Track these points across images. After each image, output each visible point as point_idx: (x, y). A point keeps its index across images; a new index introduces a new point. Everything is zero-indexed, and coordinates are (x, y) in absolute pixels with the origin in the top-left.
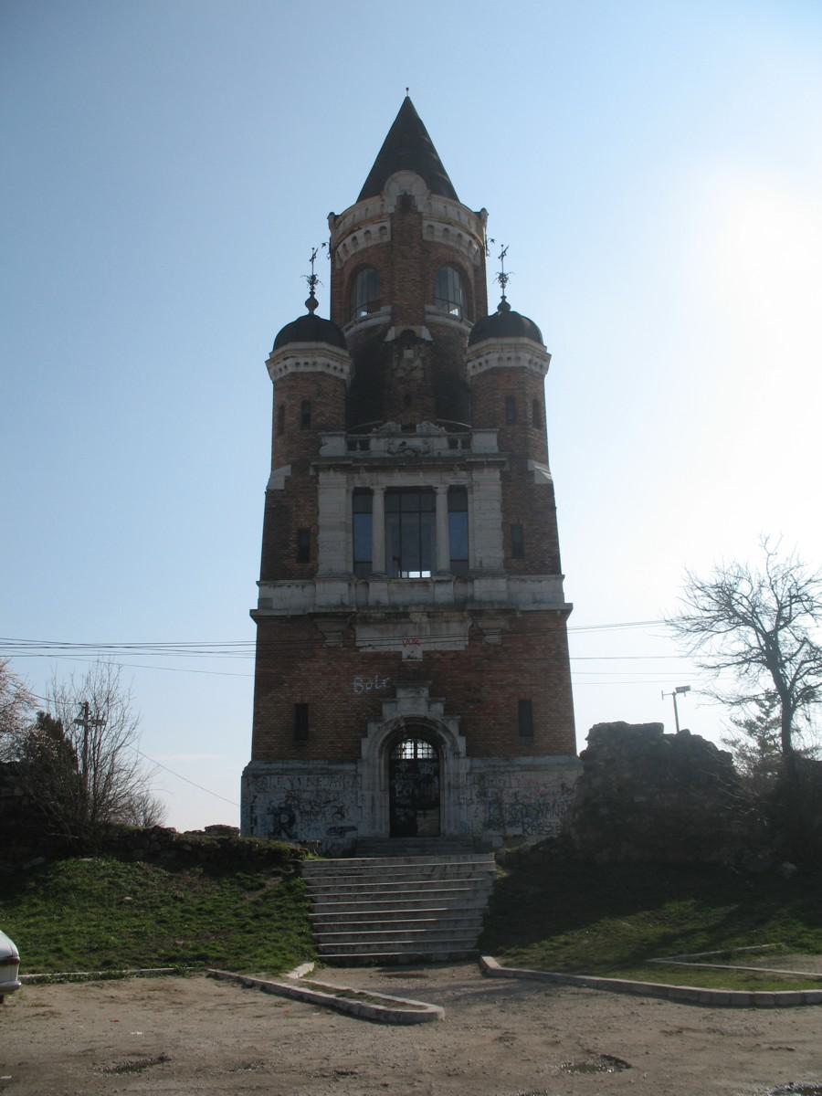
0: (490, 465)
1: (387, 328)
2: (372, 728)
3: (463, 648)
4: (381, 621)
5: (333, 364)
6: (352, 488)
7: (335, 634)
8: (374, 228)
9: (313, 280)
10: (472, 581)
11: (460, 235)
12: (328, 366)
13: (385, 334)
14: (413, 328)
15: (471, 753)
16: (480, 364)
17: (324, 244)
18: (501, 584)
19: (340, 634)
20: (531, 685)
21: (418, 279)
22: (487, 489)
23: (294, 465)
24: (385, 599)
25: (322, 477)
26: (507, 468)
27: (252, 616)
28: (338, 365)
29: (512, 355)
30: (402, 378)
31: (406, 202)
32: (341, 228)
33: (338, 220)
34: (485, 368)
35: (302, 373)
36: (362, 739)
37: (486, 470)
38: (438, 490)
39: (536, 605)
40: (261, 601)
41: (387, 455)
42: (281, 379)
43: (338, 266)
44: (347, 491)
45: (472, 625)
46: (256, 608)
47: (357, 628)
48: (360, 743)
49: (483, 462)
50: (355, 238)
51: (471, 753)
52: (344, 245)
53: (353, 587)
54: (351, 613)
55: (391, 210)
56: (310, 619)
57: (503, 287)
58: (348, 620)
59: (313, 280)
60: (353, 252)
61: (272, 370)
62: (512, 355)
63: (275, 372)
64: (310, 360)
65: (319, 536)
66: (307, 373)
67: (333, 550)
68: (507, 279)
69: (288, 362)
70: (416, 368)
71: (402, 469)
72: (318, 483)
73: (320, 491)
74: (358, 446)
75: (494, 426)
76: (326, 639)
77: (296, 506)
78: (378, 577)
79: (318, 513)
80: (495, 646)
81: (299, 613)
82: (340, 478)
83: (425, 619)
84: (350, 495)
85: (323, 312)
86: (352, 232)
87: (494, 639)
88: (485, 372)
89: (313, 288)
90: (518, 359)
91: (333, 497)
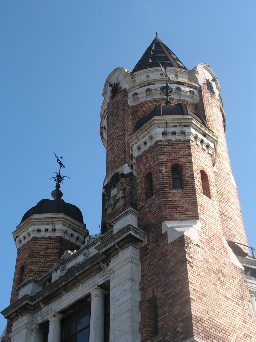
5: (43, 228)
9: (59, 179)
12: (39, 230)
28: (50, 227)
37: (120, 253)
49: (114, 246)
59: (59, 179)
64: (25, 234)
70: (118, 200)
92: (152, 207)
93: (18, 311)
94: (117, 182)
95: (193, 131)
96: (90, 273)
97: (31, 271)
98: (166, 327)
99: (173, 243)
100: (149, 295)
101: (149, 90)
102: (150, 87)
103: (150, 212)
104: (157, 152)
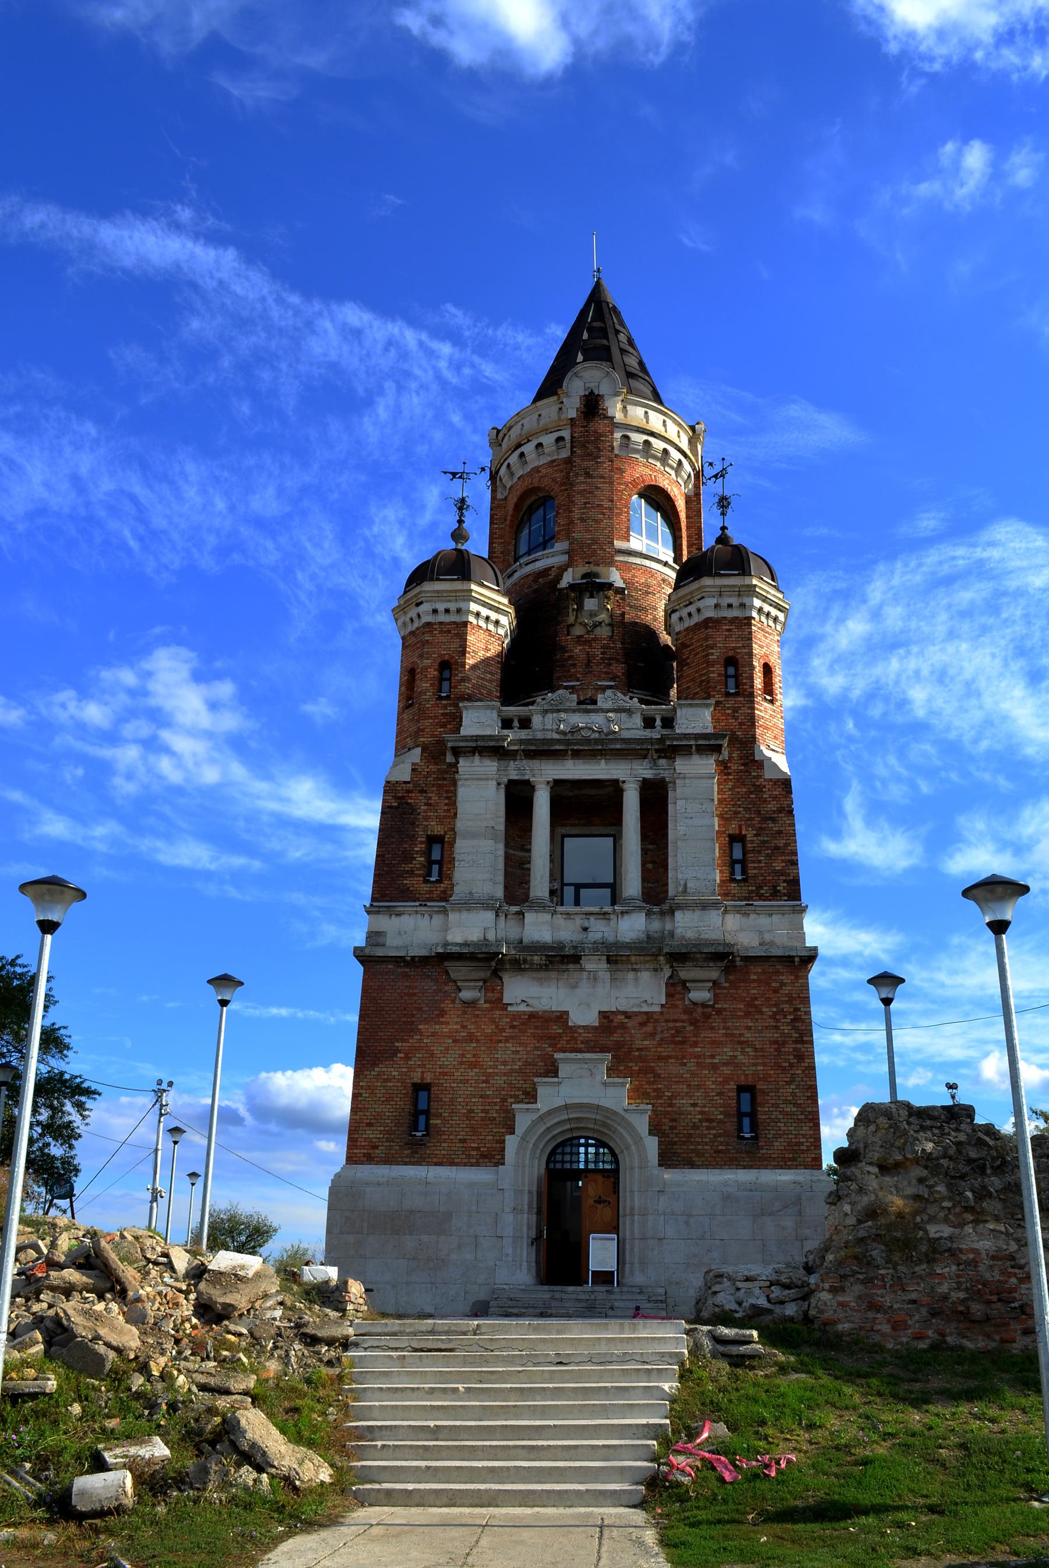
0: (702, 750)
1: (563, 569)
2: (523, 1122)
3: (657, 1009)
7: (472, 984)
8: (548, 440)
9: (462, 505)
10: (672, 912)
13: (559, 578)
14: (595, 569)
15: (668, 1158)
16: (690, 614)
17: (483, 469)
18: (714, 917)
19: (481, 984)
20: (755, 1065)
25: (463, 764)
26: (725, 753)
27: (356, 957)
29: (734, 601)
32: (505, 445)
33: (501, 435)
34: (696, 619)
35: (441, 623)
38: (625, 786)
39: (764, 948)
41: (556, 736)
42: (412, 633)
43: (499, 496)
44: (499, 784)
45: (670, 977)
47: (506, 978)
48: (504, 1141)
50: (522, 455)
51: (668, 1158)
52: (509, 465)
55: (574, 415)
56: (440, 961)
58: (493, 964)
59: (462, 505)
60: (521, 473)
61: (400, 622)
62: (734, 601)
63: (404, 624)
64: (452, 606)
65: (457, 845)
67: (477, 861)
68: (729, 504)
69: (422, 609)
70: (600, 623)
71: (577, 754)
72: (457, 772)
73: (460, 783)
74: (516, 723)
75: (708, 698)
76: (460, 990)
77: (426, 804)
78: (539, 906)
79: (456, 814)
80: (704, 1005)
81: (423, 953)
82: (489, 766)
84: (502, 792)
85: (478, 545)
86: (519, 445)
87: (700, 995)
88: (696, 624)
89: (462, 515)
94: (598, 592)
95: (757, 603)
99: (776, 782)
102: (651, 439)
103: (734, 717)
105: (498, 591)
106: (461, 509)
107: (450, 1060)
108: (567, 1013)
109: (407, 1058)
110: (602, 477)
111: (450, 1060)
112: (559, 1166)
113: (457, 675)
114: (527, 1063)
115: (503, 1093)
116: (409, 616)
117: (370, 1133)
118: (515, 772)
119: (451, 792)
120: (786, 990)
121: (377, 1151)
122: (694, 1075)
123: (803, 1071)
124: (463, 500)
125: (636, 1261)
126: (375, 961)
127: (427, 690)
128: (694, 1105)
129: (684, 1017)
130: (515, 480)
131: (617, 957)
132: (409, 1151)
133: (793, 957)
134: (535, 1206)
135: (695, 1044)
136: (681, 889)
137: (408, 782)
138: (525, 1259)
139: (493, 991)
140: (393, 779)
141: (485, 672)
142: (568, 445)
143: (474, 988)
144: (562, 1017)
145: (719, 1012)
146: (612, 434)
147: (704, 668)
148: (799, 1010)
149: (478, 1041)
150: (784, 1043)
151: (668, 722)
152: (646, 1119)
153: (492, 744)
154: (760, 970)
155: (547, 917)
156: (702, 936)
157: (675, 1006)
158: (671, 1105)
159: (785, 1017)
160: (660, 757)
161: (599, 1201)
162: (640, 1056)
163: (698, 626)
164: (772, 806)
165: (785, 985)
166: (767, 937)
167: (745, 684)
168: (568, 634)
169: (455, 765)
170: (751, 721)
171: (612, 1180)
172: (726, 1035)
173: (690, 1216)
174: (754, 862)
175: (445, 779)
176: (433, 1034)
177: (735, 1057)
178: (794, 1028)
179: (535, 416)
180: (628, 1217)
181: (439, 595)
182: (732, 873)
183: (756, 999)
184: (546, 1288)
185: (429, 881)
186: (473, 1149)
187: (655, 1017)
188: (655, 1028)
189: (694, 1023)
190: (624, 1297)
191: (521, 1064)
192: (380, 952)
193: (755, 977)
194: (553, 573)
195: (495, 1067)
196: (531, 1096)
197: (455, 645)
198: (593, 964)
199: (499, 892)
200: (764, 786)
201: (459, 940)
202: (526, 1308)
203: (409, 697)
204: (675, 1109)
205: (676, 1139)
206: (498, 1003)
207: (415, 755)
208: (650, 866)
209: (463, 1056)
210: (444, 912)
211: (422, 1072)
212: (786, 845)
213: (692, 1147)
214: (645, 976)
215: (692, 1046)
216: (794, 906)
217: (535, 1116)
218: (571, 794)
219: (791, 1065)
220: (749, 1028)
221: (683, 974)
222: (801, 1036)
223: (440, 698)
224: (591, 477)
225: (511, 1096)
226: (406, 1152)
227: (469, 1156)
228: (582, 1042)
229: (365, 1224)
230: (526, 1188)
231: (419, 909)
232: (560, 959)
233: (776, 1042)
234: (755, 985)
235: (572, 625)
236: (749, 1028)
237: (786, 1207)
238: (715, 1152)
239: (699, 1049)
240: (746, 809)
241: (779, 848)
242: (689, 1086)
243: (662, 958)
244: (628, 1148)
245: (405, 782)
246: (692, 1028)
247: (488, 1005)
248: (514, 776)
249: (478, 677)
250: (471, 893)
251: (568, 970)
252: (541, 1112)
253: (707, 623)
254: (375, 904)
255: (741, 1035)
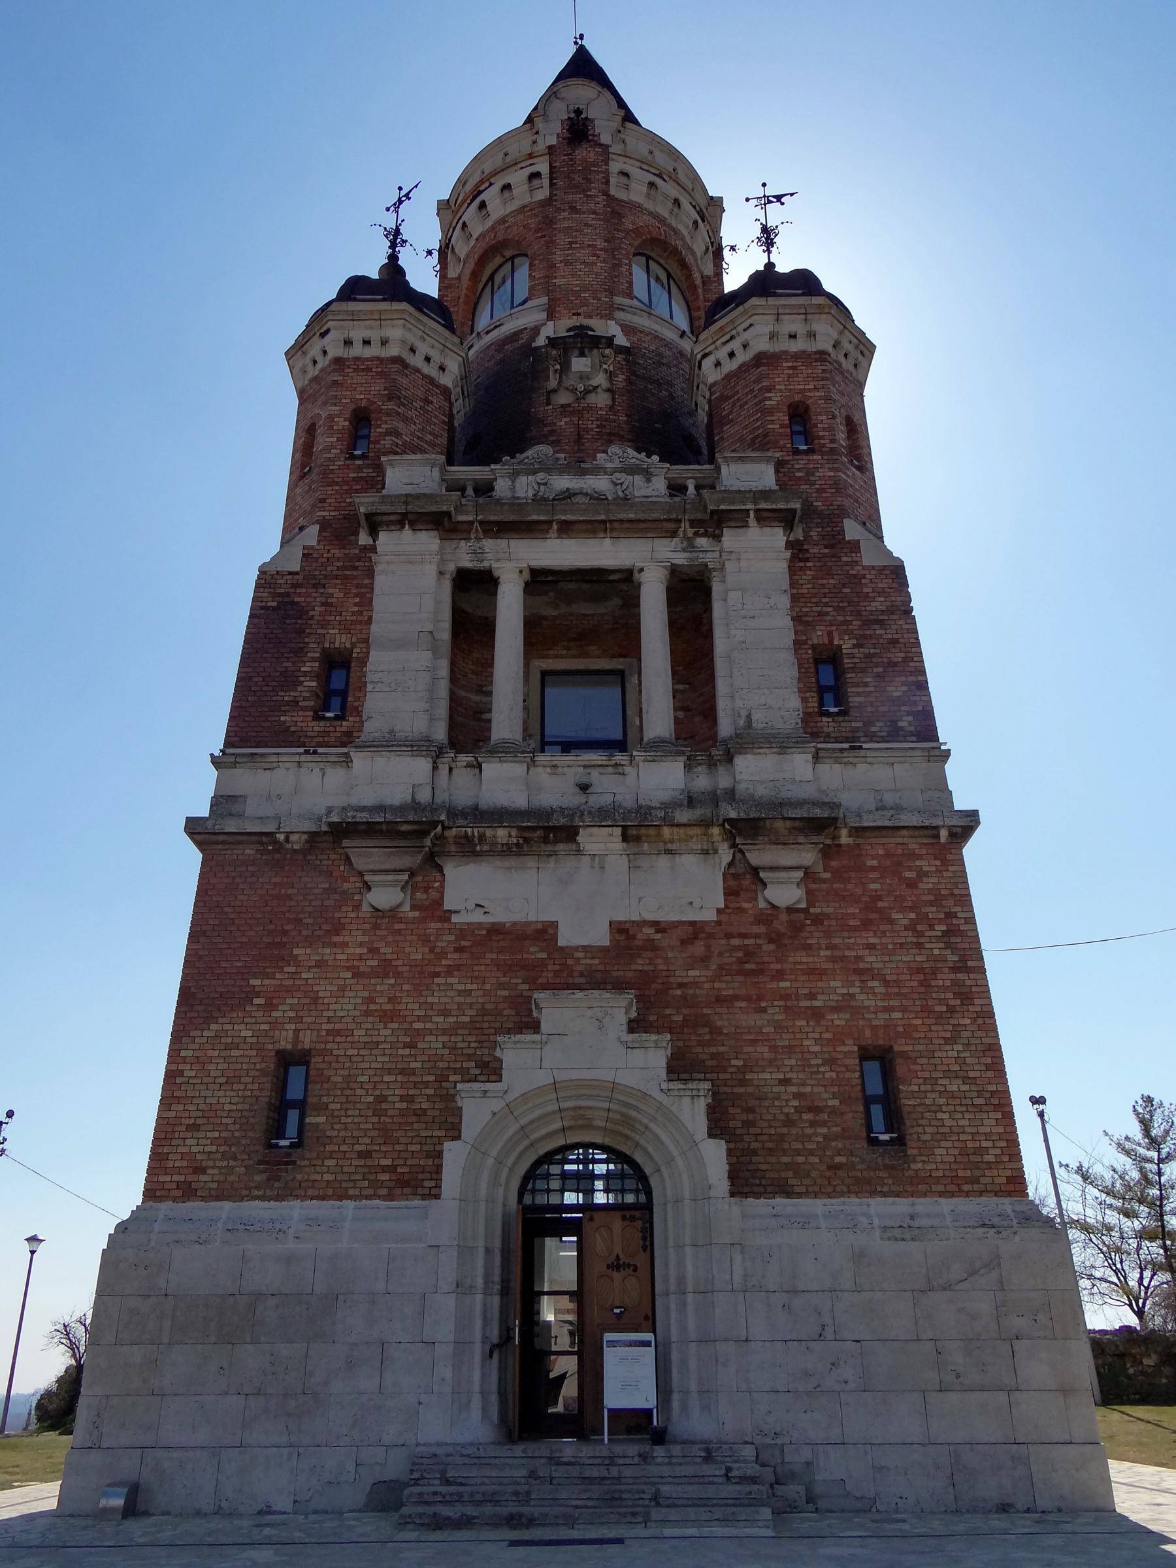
0: (764, 518)
3: (711, 916)
4: (507, 851)
6: (451, 567)
7: (390, 877)
8: (517, 178)
9: (395, 237)
10: (729, 759)
11: (677, 202)
12: (413, 350)
15: (744, 1181)
16: (732, 355)
18: (800, 764)
19: (405, 877)
20: (887, 1009)
21: (600, 244)
22: (753, 570)
23: (324, 525)
24: (518, 800)
26: (798, 533)
30: (563, 406)
31: (578, 130)
34: (742, 357)
35: (357, 359)
36: (447, 1145)
39: (888, 814)
40: (218, 802)
42: (315, 379)
43: (452, 273)
44: (441, 573)
45: (730, 864)
46: (205, 813)
48: (439, 1155)
52: (464, 225)
53: (444, 769)
54: (434, 824)
55: (553, 141)
57: (769, 252)
58: (428, 842)
59: (395, 237)
61: (296, 370)
64: (375, 336)
66: (368, 359)
70: (596, 388)
71: (567, 529)
73: (378, 569)
76: (369, 888)
77: (323, 604)
78: (505, 751)
79: (370, 618)
80: (790, 910)
83: (617, 844)
84: (447, 585)
86: (480, 193)
87: (784, 893)
90: (812, 335)
91: (410, 580)
92: (813, 475)
93: (410, 517)
94: (591, 349)
96: (646, 530)
97: (396, 433)
98: (869, 709)
100: (818, 636)
101: (652, 185)
102: (658, 181)
104: (824, 371)
105: (443, 325)
106: (393, 245)
107: (347, 1008)
108: (554, 925)
109: (270, 1006)
110: (594, 213)
111: (347, 1008)
112: (541, 1200)
113: (380, 426)
114: (483, 1012)
115: (441, 1065)
116: (309, 356)
117: (192, 1144)
118: (468, 557)
119: (366, 586)
120: (928, 883)
121: (204, 1178)
122: (778, 1026)
123: (974, 1020)
124: (397, 232)
125: (693, 1387)
126: (223, 843)
127: (332, 446)
128: (785, 1082)
129: (756, 929)
130: (472, 242)
131: (638, 828)
132: (264, 1176)
133: (937, 828)
134: (497, 1278)
135: (780, 975)
136: (742, 723)
137: (297, 573)
138: (477, 1387)
139: (426, 890)
140: (272, 569)
141: (423, 430)
142: (545, 182)
143: (393, 884)
144: (546, 933)
145: (818, 920)
146: (607, 164)
147: (757, 420)
148: (955, 915)
149: (398, 975)
150: (934, 972)
151: (707, 485)
152: (702, 1105)
153: (433, 508)
154: (881, 852)
155: (518, 769)
156: (784, 794)
157: (742, 910)
158: (743, 1082)
159: (931, 927)
160: (696, 534)
161: (617, 1265)
162: (684, 997)
163: (744, 368)
164: (878, 604)
165: (926, 874)
166: (889, 799)
167: (823, 437)
168: (548, 404)
169: (373, 549)
170: (838, 487)
171: (639, 1224)
172: (832, 959)
173: (794, 1291)
174: (857, 685)
175: (355, 568)
176: (319, 964)
177: (852, 996)
178: (949, 945)
179: (501, 155)
180: (672, 1297)
181: (354, 318)
182: (821, 704)
183: (880, 898)
184: (518, 1450)
185: (324, 718)
186: (385, 1169)
187: (708, 929)
188: (708, 948)
189: (775, 938)
190: (680, 1471)
191: (473, 1013)
192: (231, 826)
193: (875, 863)
194: (525, 336)
195: (427, 1018)
196: (492, 1070)
197: (378, 386)
198: (599, 841)
199: (440, 733)
200: (864, 576)
201: (369, 801)
202: (479, 1503)
203: (303, 467)
204: (750, 1090)
205: (755, 1145)
206: (435, 910)
207: (311, 535)
208: (681, 714)
209: (371, 1000)
210: (347, 761)
211: (297, 1031)
212: (906, 660)
213: (785, 1159)
214: (689, 862)
215: (773, 978)
216: (929, 749)
217: (497, 1105)
218: (555, 613)
219: (951, 1010)
220: (871, 947)
221: (756, 857)
222: (963, 959)
223: (353, 457)
224: (577, 211)
225: (456, 1071)
226: (258, 1178)
227: (375, 1184)
228: (582, 975)
229: (167, 1324)
230: (481, 1243)
231: (303, 758)
232: (545, 833)
233: (920, 970)
234: (876, 875)
235: (555, 391)
236: (871, 947)
237: (973, 1273)
238: (830, 1168)
239: (787, 984)
240: (838, 609)
241: (895, 664)
242: (773, 1049)
243: (716, 831)
244: (670, 1161)
245: (290, 573)
246: (772, 947)
247: (417, 914)
248: (467, 562)
249: (412, 434)
250: (392, 732)
251: (554, 854)
252: (510, 1097)
253: (761, 359)
254: (229, 751)
255: (859, 958)
